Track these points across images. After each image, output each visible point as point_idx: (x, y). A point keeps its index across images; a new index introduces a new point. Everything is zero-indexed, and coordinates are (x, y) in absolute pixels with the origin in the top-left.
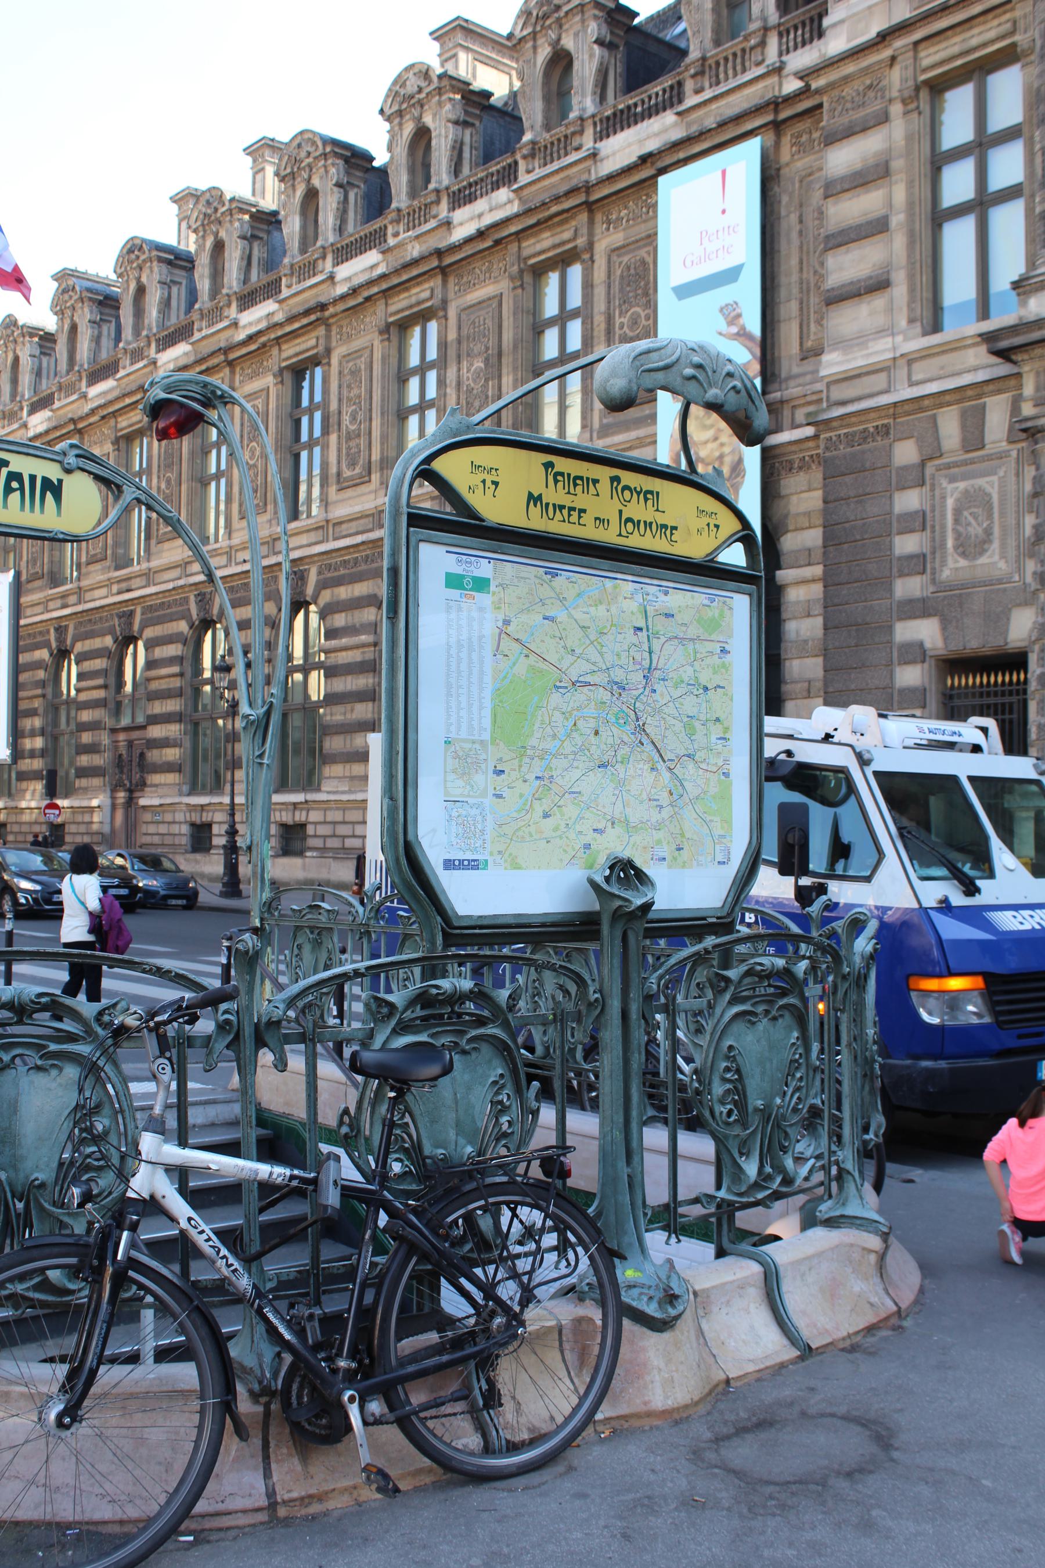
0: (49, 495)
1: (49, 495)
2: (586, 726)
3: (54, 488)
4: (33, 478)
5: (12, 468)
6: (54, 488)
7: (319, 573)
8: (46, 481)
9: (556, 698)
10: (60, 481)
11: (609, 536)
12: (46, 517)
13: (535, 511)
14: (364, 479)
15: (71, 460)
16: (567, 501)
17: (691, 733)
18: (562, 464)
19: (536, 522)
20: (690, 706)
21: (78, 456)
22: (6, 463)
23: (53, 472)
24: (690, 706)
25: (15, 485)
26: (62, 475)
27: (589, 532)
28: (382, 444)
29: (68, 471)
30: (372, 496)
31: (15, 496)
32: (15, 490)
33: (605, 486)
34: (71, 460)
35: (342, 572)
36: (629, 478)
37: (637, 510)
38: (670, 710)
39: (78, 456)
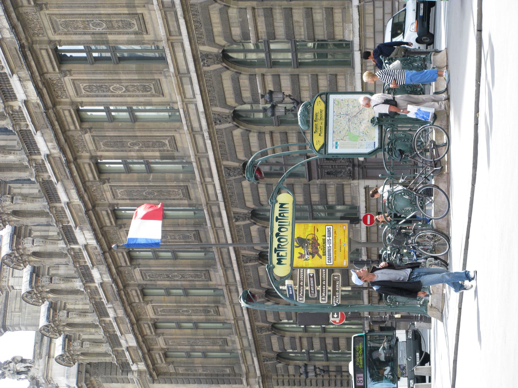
2: (355, 126)
3: (282, 205)
4: (280, 210)
5: (278, 216)
6: (282, 205)
7: (204, 44)
8: (280, 207)
9: (351, 131)
11: (323, 122)
12: (290, 207)
13: (321, 135)
14: (141, 19)
16: (319, 129)
17: (355, 107)
18: (314, 131)
19: (323, 134)
20: (351, 107)
22: (277, 217)
23: (277, 206)
24: (351, 107)
25: (282, 215)
27: (323, 125)
28: (117, 7)
29: (277, 202)
30: (152, 12)
33: (316, 123)
35: (203, 30)
36: (314, 119)
37: (319, 117)
38: (352, 110)
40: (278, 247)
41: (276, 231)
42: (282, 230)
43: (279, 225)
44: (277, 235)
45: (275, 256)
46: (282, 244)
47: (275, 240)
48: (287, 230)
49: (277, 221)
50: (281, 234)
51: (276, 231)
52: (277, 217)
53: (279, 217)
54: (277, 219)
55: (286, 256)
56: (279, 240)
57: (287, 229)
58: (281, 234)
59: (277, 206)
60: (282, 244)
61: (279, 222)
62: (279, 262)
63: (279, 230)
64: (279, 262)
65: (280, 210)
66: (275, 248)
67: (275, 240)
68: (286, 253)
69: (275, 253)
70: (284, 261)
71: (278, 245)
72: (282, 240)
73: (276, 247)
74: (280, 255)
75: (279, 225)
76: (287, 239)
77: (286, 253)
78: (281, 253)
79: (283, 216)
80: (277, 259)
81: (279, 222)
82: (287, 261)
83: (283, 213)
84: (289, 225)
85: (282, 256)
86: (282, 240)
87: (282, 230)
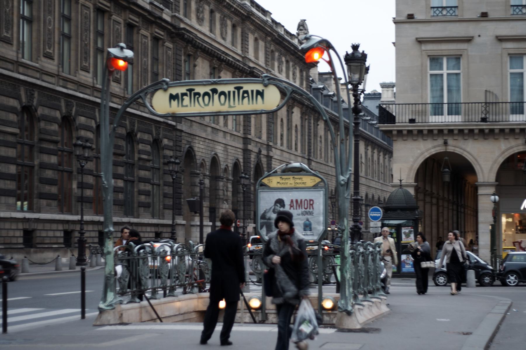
0: (259, 97)
3: (260, 94)
4: (252, 91)
6: (260, 94)
10: (263, 90)
12: (259, 105)
15: (266, 82)
21: (268, 80)
22: (242, 88)
23: (260, 87)
25: (246, 95)
29: (266, 86)
31: (246, 100)
34: (266, 82)
39: (268, 80)
40: (196, 94)
41: (220, 88)
43: (229, 92)
44: (214, 91)
45: (183, 90)
46: (201, 99)
47: (208, 89)
48: (222, 104)
49: (235, 88)
50: (216, 97)
51: (220, 88)
52: (242, 88)
53: (241, 91)
55: (182, 106)
56: (206, 94)
57: (224, 104)
59: (260, 87)
60: (201, 99)
61: (234, 92)
62: (172, 97)
63: (223, 93)
64: (172, 97)
65: (252, 91)
67: (208, 89)
68: (187, 106)
69: (187, 90)
70: (174, 103)
71: (199, 94)
72: (206, 98)
73: (196, 91)
74: (185, 97)
75: (229, 92)
76: (208, 105)
77: (187, 106)
79: (243, 97)
80: (177, 94)
81: (234, 92)
82: (175, 108)
83: (248, 96)
84: (230, 106)
85: (183, 100)
86: (206, 98)
87: (223, 97)
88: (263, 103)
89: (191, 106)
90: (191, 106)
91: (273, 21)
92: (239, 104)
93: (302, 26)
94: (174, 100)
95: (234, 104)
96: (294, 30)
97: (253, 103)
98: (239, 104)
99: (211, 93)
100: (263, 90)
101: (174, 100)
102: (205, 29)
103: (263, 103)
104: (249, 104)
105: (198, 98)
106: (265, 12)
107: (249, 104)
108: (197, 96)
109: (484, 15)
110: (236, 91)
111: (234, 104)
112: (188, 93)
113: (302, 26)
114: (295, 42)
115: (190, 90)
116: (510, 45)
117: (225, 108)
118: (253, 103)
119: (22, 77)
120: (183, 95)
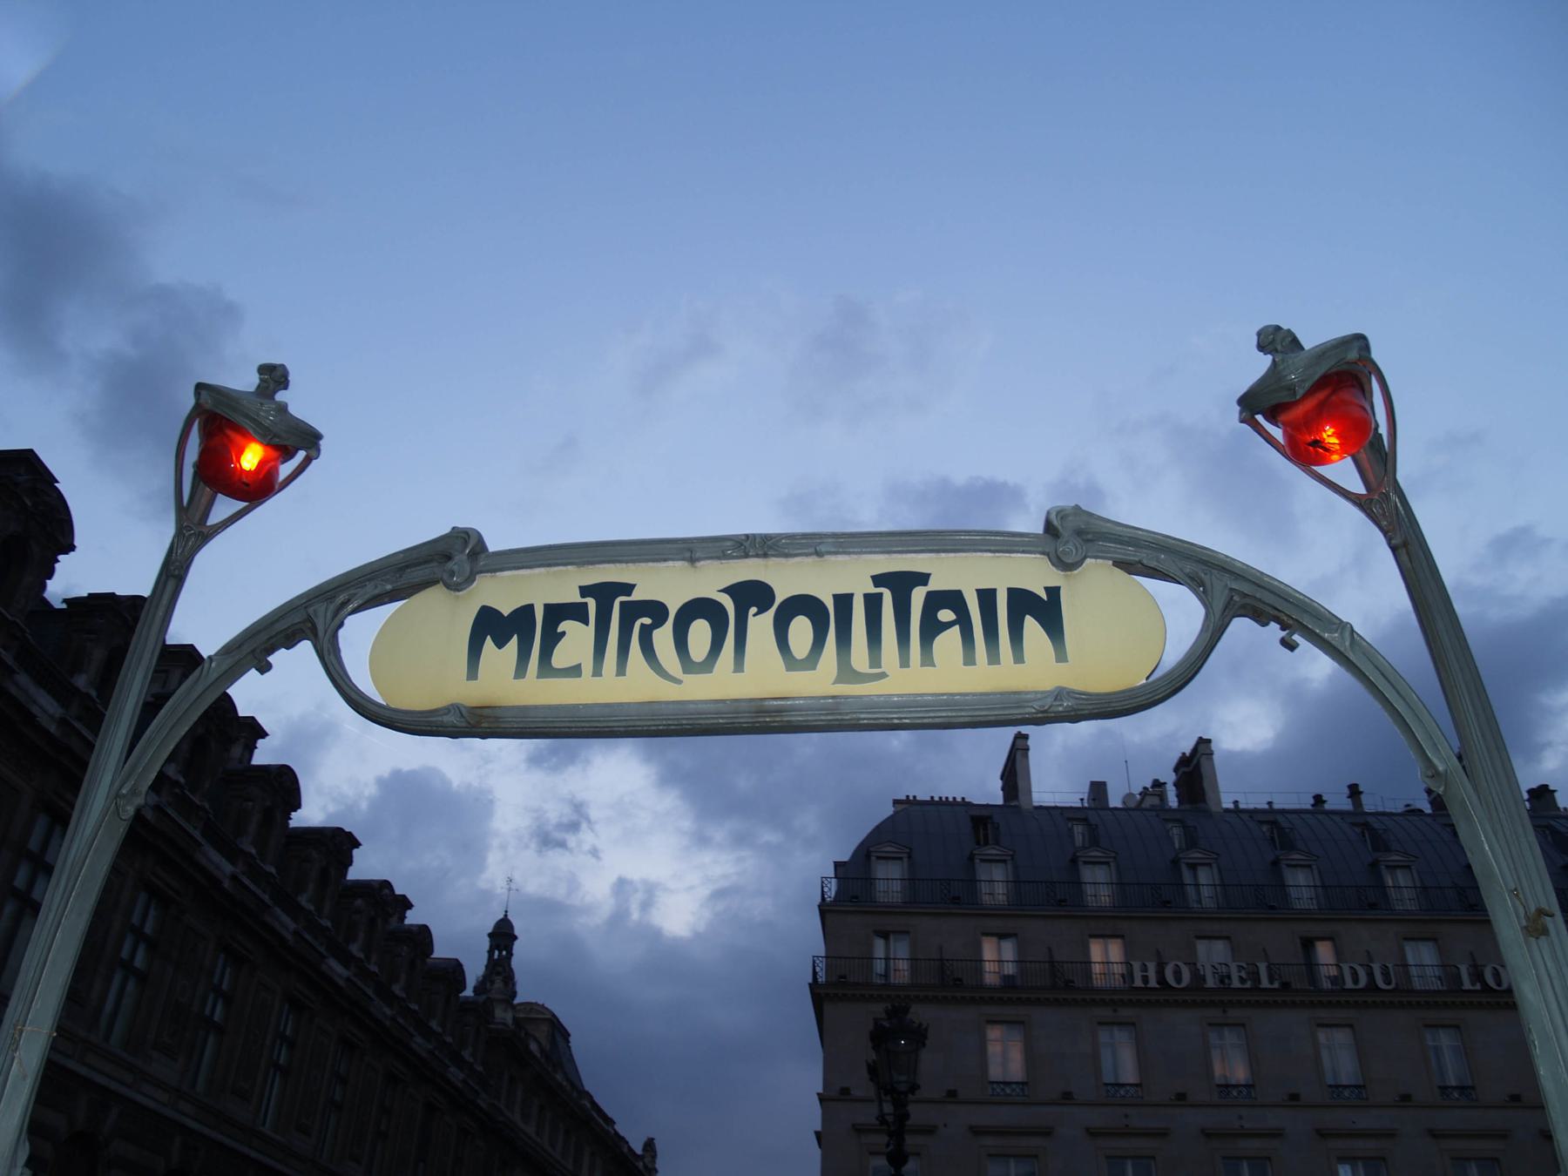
0: (1030, 624)
1: (1030, 624)
5: (934, 585)
10: (1054, 592)
12: (1033, 666)
23: (1035, 575)
25: (946, 615)
26: (1054, 577)
31: (950, 640)
32: (948, 625)
40: (632, 611)
41: (787, 580)
42: (801, 629)
43: (844, 602)
45: (564, 586)
46: (663, 638)
49: (878, 580)
50: (761, 625)
52: (923, 579)
53: (918, 596)
54: (901, 584)
56: (700, 608)
58: (761, 625)
60: (663, 638)
61: (873, 603)
62: (490, 626)
64: (490, 626)
66: (628, 589)
67: (711, 581)
68: (575, 671)
69: (585, 591)
70: (499, 658)
71: (657, 611)
72: (700, 632)
73: (636, 596)
74: (566, 626)
75: (844, 602)
77: (575, 671)
78: (577, 639)
79: (932, 629)
80: (529, 609)
81: (873, 603)
83: (964, 621)
84: (846, 672)
85: (552, 638)
86: (700, 632)
87: (801, 629)
88: (1061, 656)
89: (597, 672)
90: (597, 672)
91: (616, 1133)
92: (905, 662)
93: (650, 1145)
94: (500, 643)
95: (875, 660)
96: (639, 1151)
97: (994, 657)
98: (905, 662)
99: (728, 602)
100: (1054, 592)
101: (500, 643)
102: (530, 1130)
103: (1061, 656)
104: (969, 659)
105: (646, 634)
106: (610, 1122)
107: (969, 659)
108: (647, 621)
109: (952, 1094)
110: (887, 596)
111: (875, 660)
112: (592, 603)
113: (650, 1145)
114: (640, 1165)
115: (605, 593)
116: (989, 1141)
117: (820, 682)
118: (994, 657)
119: (254, 1154)
120: (556, 613)
